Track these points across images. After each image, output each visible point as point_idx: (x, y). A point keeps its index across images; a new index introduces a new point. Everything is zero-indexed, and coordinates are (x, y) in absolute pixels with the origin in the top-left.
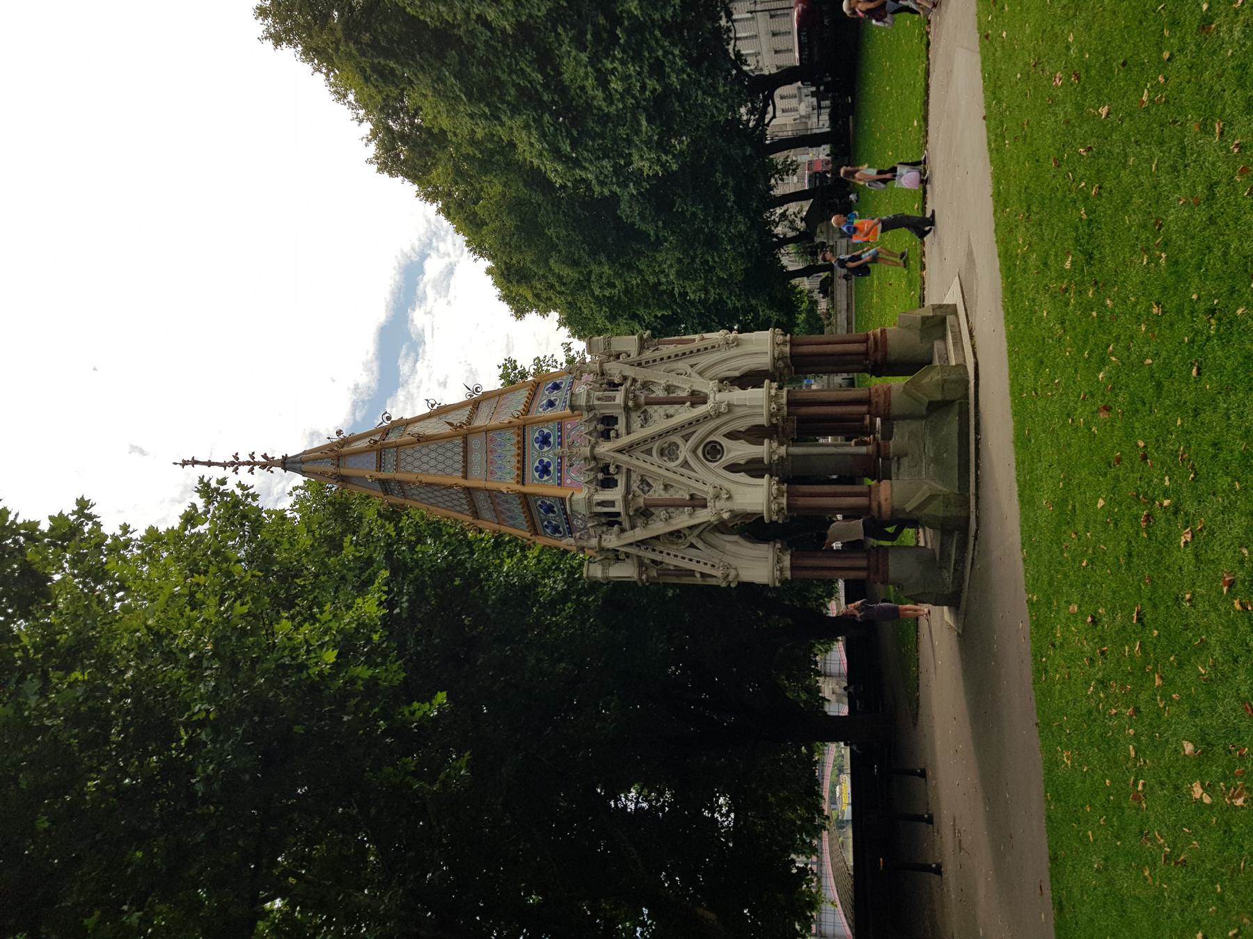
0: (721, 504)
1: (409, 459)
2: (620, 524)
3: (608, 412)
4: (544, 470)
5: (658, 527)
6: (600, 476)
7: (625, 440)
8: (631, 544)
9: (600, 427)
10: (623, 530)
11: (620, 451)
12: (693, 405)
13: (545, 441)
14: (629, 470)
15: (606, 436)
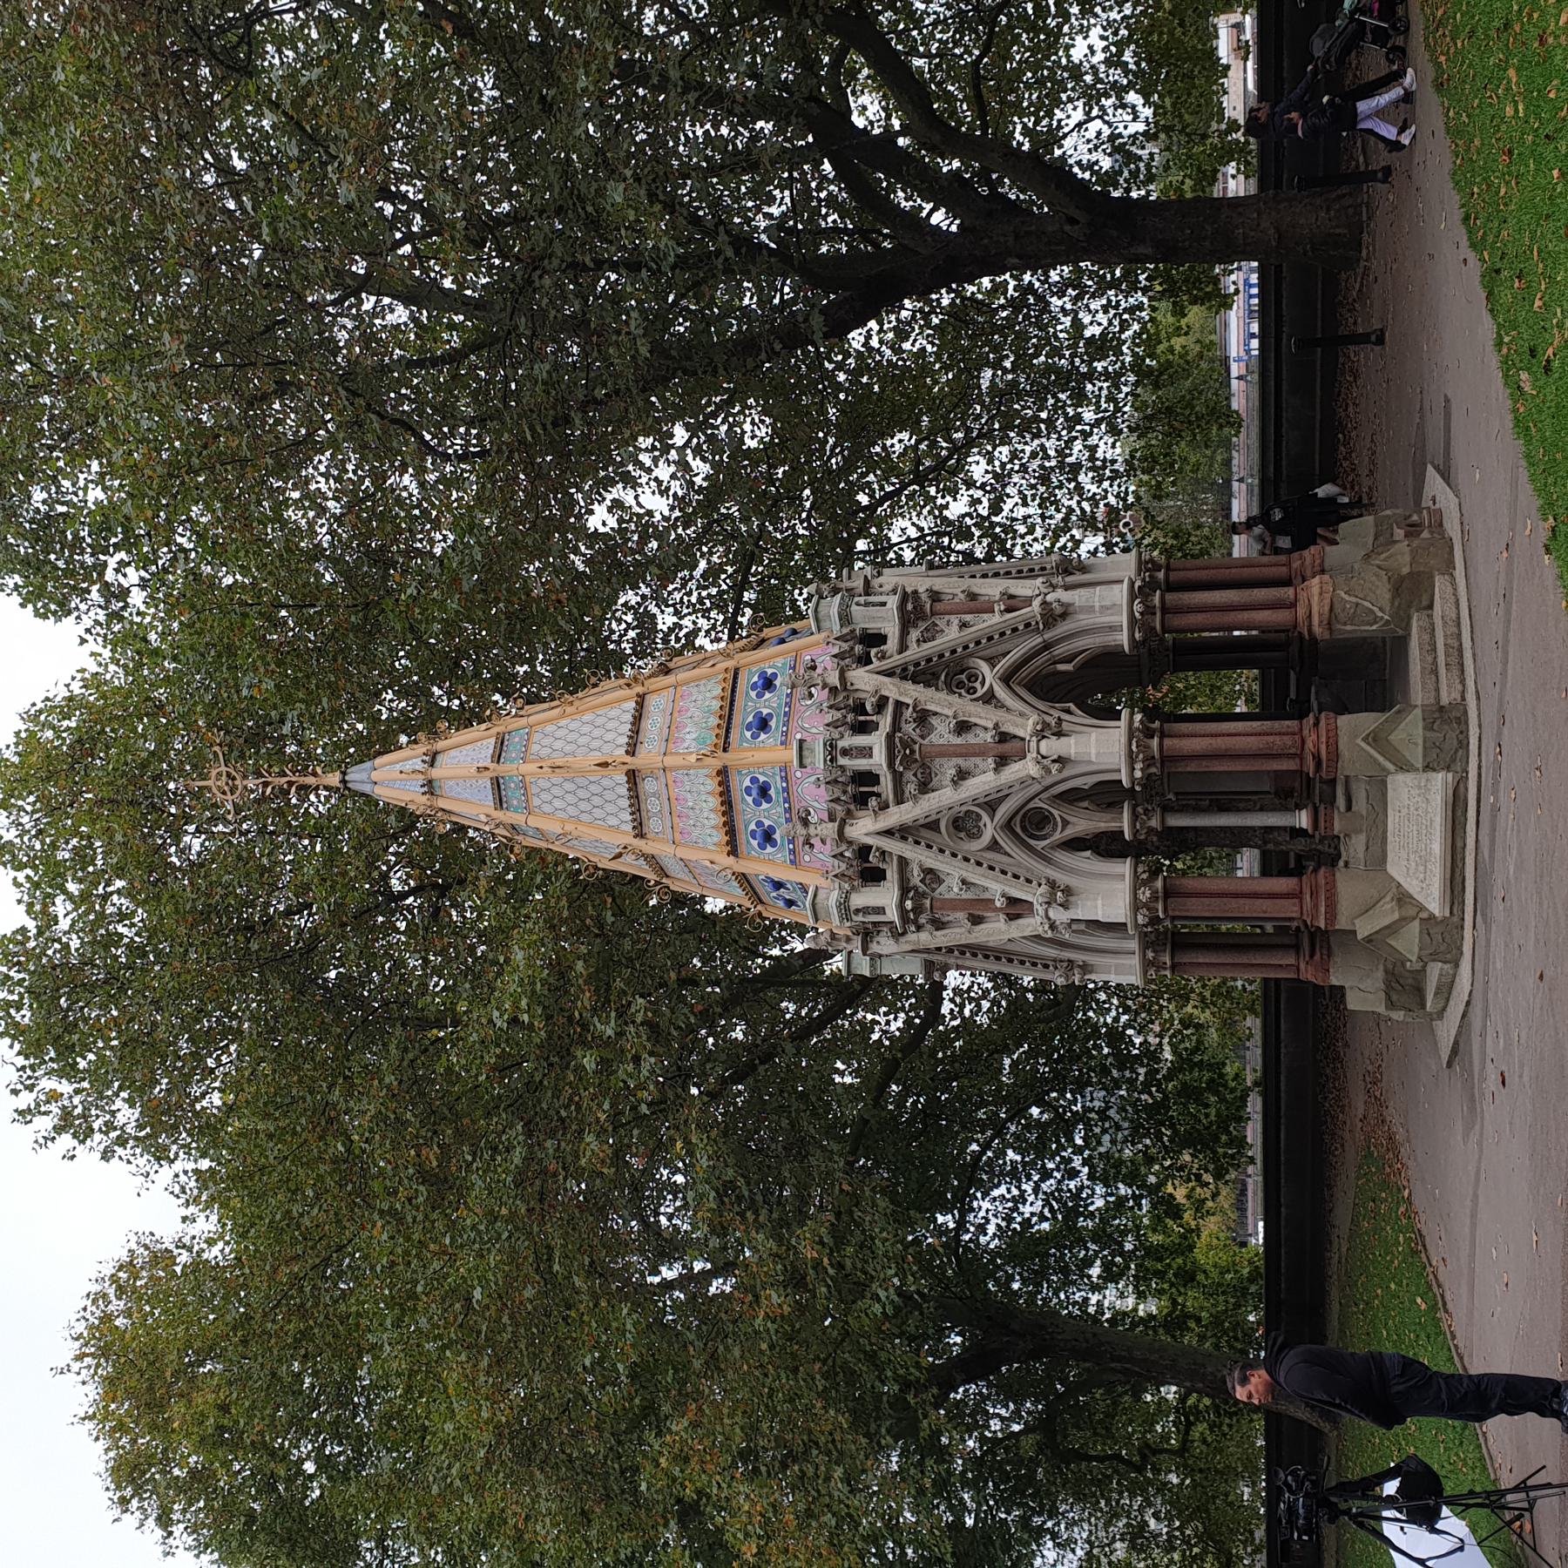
0: (1051, 746)
1: (546, 741)
2: (878, 795)
3: (873, 626)
4: (763, 724)
5: (944, 798)
6: (850, 717)
7: (897, 660)
8: (888, 833)
9: (858, 649)
10: (884, 806)
11: (889, 673)
12: (1009, 610)
13: (768, 683)
14: (899, 705)
15: (865, 660)
